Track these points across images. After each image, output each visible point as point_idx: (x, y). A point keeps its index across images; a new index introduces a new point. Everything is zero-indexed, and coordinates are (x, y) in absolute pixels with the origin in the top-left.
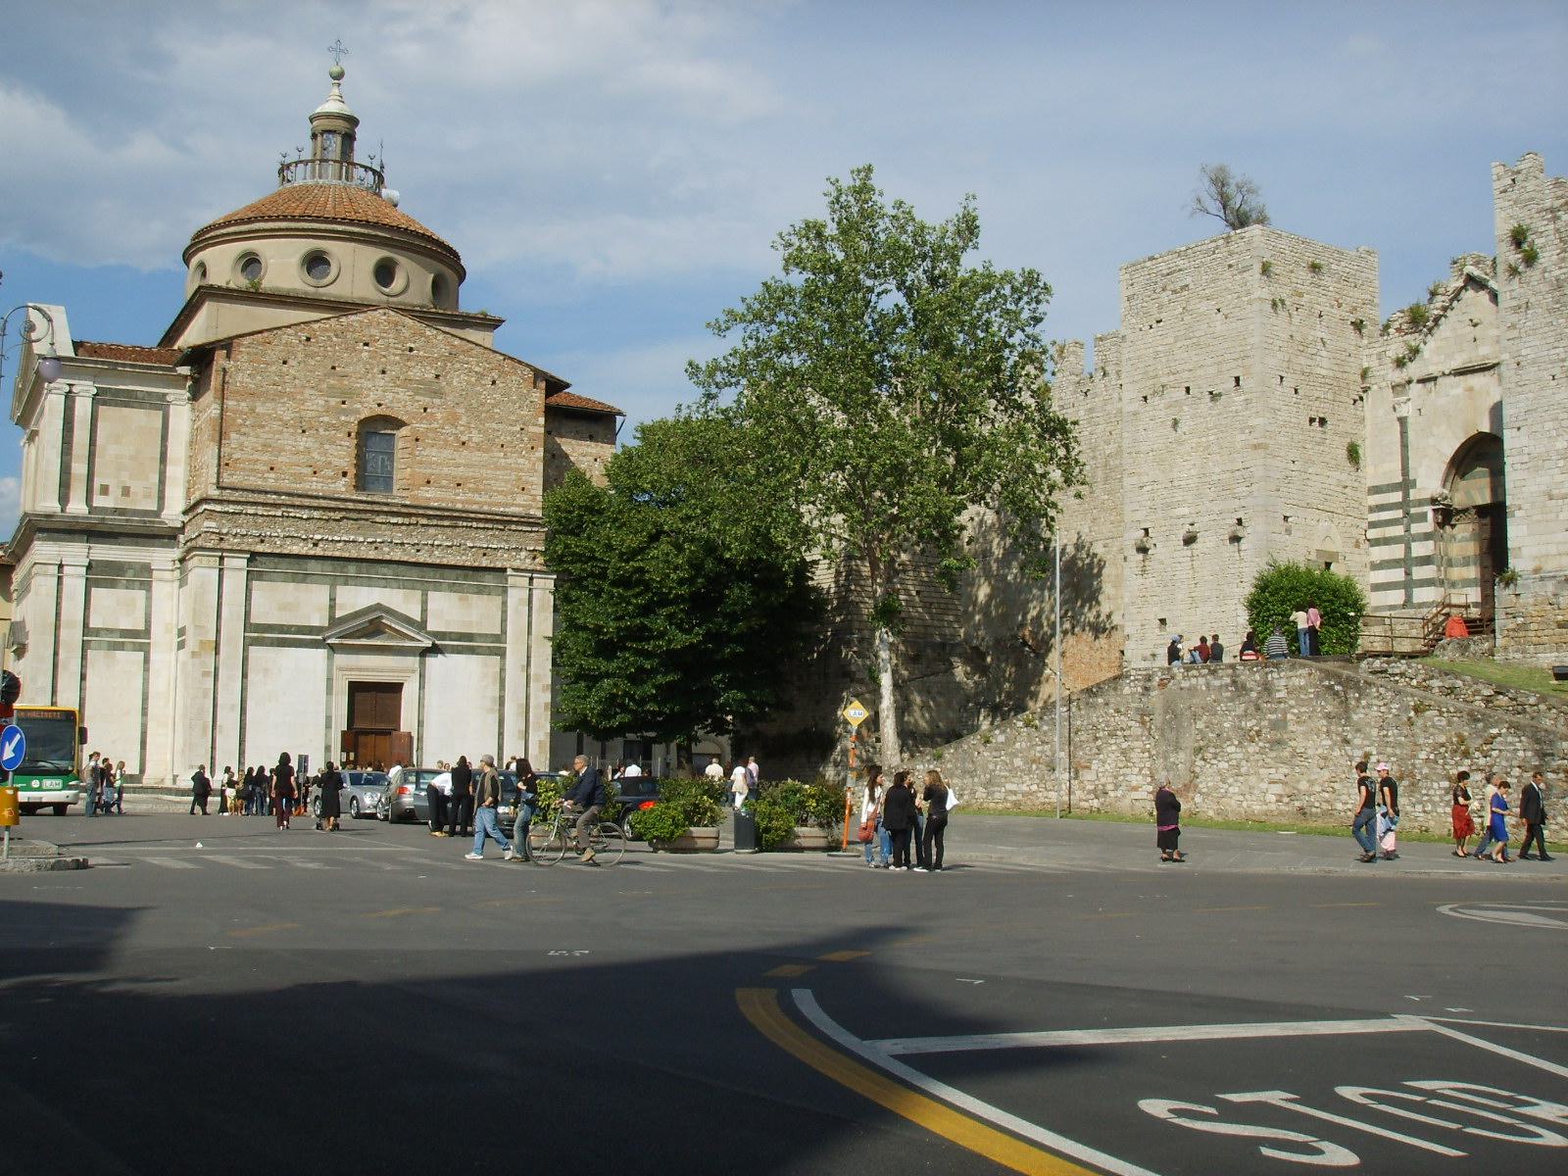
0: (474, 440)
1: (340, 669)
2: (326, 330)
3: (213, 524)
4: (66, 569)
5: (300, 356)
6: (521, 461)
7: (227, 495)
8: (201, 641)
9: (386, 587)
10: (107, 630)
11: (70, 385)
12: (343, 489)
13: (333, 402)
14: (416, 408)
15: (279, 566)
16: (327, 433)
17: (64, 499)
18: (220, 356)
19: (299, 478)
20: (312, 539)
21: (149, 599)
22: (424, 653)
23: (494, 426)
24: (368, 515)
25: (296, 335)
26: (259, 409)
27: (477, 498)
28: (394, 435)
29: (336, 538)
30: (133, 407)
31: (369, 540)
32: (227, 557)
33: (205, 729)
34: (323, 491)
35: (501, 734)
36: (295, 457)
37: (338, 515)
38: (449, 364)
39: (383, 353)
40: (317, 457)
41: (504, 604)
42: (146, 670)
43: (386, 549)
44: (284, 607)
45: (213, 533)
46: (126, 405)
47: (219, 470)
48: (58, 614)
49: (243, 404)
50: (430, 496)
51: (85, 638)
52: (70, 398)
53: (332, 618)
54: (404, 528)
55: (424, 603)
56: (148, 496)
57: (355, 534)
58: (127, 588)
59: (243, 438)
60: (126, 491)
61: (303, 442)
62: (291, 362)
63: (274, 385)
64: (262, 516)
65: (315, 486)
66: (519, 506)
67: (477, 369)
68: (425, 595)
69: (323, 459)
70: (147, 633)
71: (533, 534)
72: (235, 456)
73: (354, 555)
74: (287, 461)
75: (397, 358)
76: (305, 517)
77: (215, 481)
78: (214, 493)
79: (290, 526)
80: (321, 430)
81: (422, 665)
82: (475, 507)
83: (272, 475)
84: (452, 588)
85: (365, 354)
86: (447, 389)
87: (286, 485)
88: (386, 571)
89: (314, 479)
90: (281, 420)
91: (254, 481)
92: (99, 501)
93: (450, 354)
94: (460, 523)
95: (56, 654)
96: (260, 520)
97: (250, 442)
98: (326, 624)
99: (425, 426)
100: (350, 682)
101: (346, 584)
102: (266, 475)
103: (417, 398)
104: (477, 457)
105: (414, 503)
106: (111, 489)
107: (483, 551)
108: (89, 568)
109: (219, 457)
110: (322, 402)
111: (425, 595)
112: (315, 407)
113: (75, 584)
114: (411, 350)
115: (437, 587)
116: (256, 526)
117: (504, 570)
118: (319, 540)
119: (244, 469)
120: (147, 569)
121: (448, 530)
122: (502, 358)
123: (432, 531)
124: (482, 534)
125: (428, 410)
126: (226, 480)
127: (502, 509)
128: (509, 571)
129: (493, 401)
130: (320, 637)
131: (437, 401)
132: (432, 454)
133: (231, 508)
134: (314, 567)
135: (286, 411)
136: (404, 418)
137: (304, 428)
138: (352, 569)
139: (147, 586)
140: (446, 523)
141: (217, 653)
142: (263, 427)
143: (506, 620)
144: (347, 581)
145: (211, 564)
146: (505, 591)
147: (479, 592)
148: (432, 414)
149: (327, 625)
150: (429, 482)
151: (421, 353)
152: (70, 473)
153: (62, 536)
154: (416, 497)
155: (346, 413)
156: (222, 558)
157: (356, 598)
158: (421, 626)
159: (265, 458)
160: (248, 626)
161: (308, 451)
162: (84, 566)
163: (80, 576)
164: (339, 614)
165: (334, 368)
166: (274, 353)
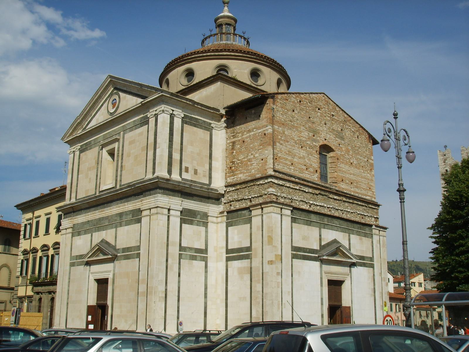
0: (355, 163)
1: (326, 273)
2: (306, 99)
3: (274, 190)
4: (171, 211)
5: (298, 109)
6: (368, 175)
7: (277, 174)
8: (275, 254)
9: (337, 231)
10: (189, 248)
11: (173, 111)
12: (317, 179)
13: (311, 134)
14: (336, 143)
15: (301, 216)
16: (310, 150)
17: (170, 172)
18: (270, 101)
19: (301, 171)
20: (309, 203)
21: (207, 232)
23: (360, 157)
24: (327, 194)
25: (296, 98)
26: (286, 133)
27: (357, 190)
28: (327, 155)
29: (318, 204)
30: (198, 128)
31: (328, 206)
33: (278, 305)
34: (310, 179)
35: (375, 307)
36: (300, 159)
37: (317, 192)
38: (344, 125)
39: (325, 115)
40: (307, 161)
41: (372, 242)
42: (206, 272)
43: (333, 212)
44: (305, 238)
45: (275, 195)
46: (195, 126)
47: (274, 161)
48: (168, 237)
49: (280, 129)
50: (343, 187)
51: (180, 252)
52: (172, 116)
54: (338, 201)
55: (349, 240)
56: (204, 176)
57: (324, 203)
58: (197, 225)
59: (281, 146)
60: (196, 172)
61: (303, 153)
62: (296, 112)
63: (290, 121)
64: (292, 188)
65: (306, 176)
66: (369, 196)
67: (353, 130)
68: (349, 236)
69: (309, 163)
70: (205, 251)
71: (375, 210)
72: (279, 155)
73: (323, 212)
74: (297, 161)
75: (329, 118)
76: (307, 191)
77: (272, 167)
78: (273, 173)
79: (301, 195)
80: (308, 149)
81: (350, 271)
82: (357, 195)
83: (293, 168)
84: (358, 234)
85: (319, 114)
86: (345, 137)
87: (297, 174)
88: (336, 222)
89: (307, 172)
90: (294, 140)
91: (286, 170)
92: (185, 176)
93: (345, 121)
94: (356, 202)
95: (167, 261)
96: (291, 190)
97: (283, 148)
98: (319, 249)
99: (340, 153)
100: (328, 280)
101: (324, 228)
102: (290, 167)
103: (337, 139)
104: (356, 171)
105: (340, 190)
106: (190, 170)
107: (361, 216)
108: (181, 212)
109: (273, 155)
110: (307, 134)
111: (349, 236)
112: (304, 136)
113: (175, 221)
114: (333, 115)
116: (289, 193)
117: (371, 226)
118: (312, 204)
119: (282, 162)
120: (205, 215)
121: (351, 204)
122: (359, 126)
123: (346, 204)
124: (361, 208)
125: (340, 146)
126: (277, 167)
127: (364, 197)
128: (374, 227)
129: (358, 146)
130: (317, 255)
131: (343, 142)
132: (342, 165)
133: (281, 182)
134: (313, 218)
135: (295, 135)
136: (333, 148)
137: (302, 145)
138: (326, 220)
139: (206, 225)
140: (351, 201)
141: (282, 262)
142: (288, 142)
143: (373, 251)
144: (325, 226)
146: (372, 237)
147: (365, 236)
148: (342, 148)
149: (319, 249)
150: (342, 180)
151: (336, 118)
152: (172, 158)
153: (172, 193)
154: (340, 187)
155: (315, 141)
159: (290, 158)
161: (304, 158)
162: (179, 211)
163: (177, 216)
164: (323, 244)
165: (310, 118)
166: (289, 106)
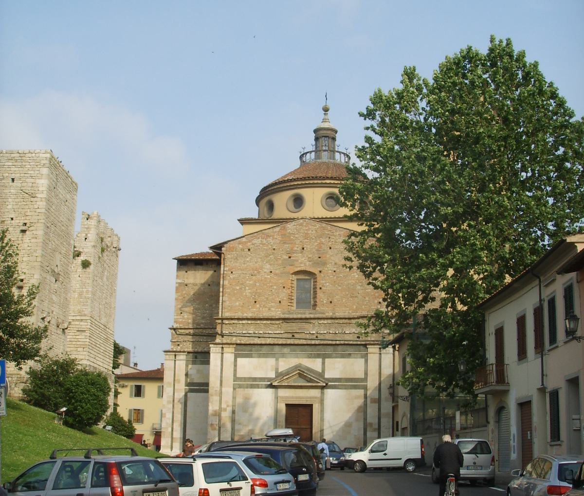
22: (323, 388)
32: (226, 347)
53: (277, 372)
55: (323, 363)
81: (322, 393)
98: (274, 376)
115: (330, 356)
138: (286, 350)
144: (283, 356)
145: (217, 351)
146: (365, 357)
149: (274, 377)
156: (222, 348)
157: (286, 363)
158: (321, 375)
160: (236, 378)
